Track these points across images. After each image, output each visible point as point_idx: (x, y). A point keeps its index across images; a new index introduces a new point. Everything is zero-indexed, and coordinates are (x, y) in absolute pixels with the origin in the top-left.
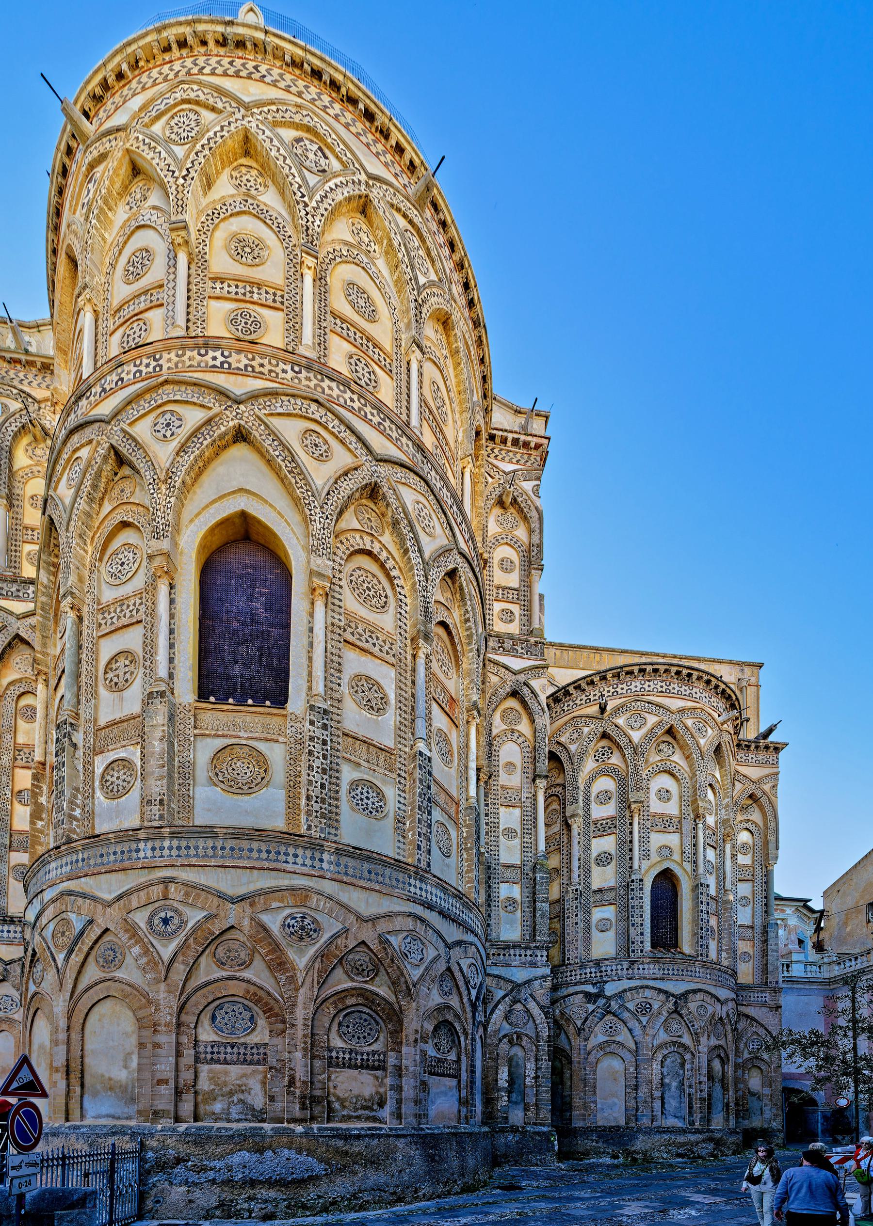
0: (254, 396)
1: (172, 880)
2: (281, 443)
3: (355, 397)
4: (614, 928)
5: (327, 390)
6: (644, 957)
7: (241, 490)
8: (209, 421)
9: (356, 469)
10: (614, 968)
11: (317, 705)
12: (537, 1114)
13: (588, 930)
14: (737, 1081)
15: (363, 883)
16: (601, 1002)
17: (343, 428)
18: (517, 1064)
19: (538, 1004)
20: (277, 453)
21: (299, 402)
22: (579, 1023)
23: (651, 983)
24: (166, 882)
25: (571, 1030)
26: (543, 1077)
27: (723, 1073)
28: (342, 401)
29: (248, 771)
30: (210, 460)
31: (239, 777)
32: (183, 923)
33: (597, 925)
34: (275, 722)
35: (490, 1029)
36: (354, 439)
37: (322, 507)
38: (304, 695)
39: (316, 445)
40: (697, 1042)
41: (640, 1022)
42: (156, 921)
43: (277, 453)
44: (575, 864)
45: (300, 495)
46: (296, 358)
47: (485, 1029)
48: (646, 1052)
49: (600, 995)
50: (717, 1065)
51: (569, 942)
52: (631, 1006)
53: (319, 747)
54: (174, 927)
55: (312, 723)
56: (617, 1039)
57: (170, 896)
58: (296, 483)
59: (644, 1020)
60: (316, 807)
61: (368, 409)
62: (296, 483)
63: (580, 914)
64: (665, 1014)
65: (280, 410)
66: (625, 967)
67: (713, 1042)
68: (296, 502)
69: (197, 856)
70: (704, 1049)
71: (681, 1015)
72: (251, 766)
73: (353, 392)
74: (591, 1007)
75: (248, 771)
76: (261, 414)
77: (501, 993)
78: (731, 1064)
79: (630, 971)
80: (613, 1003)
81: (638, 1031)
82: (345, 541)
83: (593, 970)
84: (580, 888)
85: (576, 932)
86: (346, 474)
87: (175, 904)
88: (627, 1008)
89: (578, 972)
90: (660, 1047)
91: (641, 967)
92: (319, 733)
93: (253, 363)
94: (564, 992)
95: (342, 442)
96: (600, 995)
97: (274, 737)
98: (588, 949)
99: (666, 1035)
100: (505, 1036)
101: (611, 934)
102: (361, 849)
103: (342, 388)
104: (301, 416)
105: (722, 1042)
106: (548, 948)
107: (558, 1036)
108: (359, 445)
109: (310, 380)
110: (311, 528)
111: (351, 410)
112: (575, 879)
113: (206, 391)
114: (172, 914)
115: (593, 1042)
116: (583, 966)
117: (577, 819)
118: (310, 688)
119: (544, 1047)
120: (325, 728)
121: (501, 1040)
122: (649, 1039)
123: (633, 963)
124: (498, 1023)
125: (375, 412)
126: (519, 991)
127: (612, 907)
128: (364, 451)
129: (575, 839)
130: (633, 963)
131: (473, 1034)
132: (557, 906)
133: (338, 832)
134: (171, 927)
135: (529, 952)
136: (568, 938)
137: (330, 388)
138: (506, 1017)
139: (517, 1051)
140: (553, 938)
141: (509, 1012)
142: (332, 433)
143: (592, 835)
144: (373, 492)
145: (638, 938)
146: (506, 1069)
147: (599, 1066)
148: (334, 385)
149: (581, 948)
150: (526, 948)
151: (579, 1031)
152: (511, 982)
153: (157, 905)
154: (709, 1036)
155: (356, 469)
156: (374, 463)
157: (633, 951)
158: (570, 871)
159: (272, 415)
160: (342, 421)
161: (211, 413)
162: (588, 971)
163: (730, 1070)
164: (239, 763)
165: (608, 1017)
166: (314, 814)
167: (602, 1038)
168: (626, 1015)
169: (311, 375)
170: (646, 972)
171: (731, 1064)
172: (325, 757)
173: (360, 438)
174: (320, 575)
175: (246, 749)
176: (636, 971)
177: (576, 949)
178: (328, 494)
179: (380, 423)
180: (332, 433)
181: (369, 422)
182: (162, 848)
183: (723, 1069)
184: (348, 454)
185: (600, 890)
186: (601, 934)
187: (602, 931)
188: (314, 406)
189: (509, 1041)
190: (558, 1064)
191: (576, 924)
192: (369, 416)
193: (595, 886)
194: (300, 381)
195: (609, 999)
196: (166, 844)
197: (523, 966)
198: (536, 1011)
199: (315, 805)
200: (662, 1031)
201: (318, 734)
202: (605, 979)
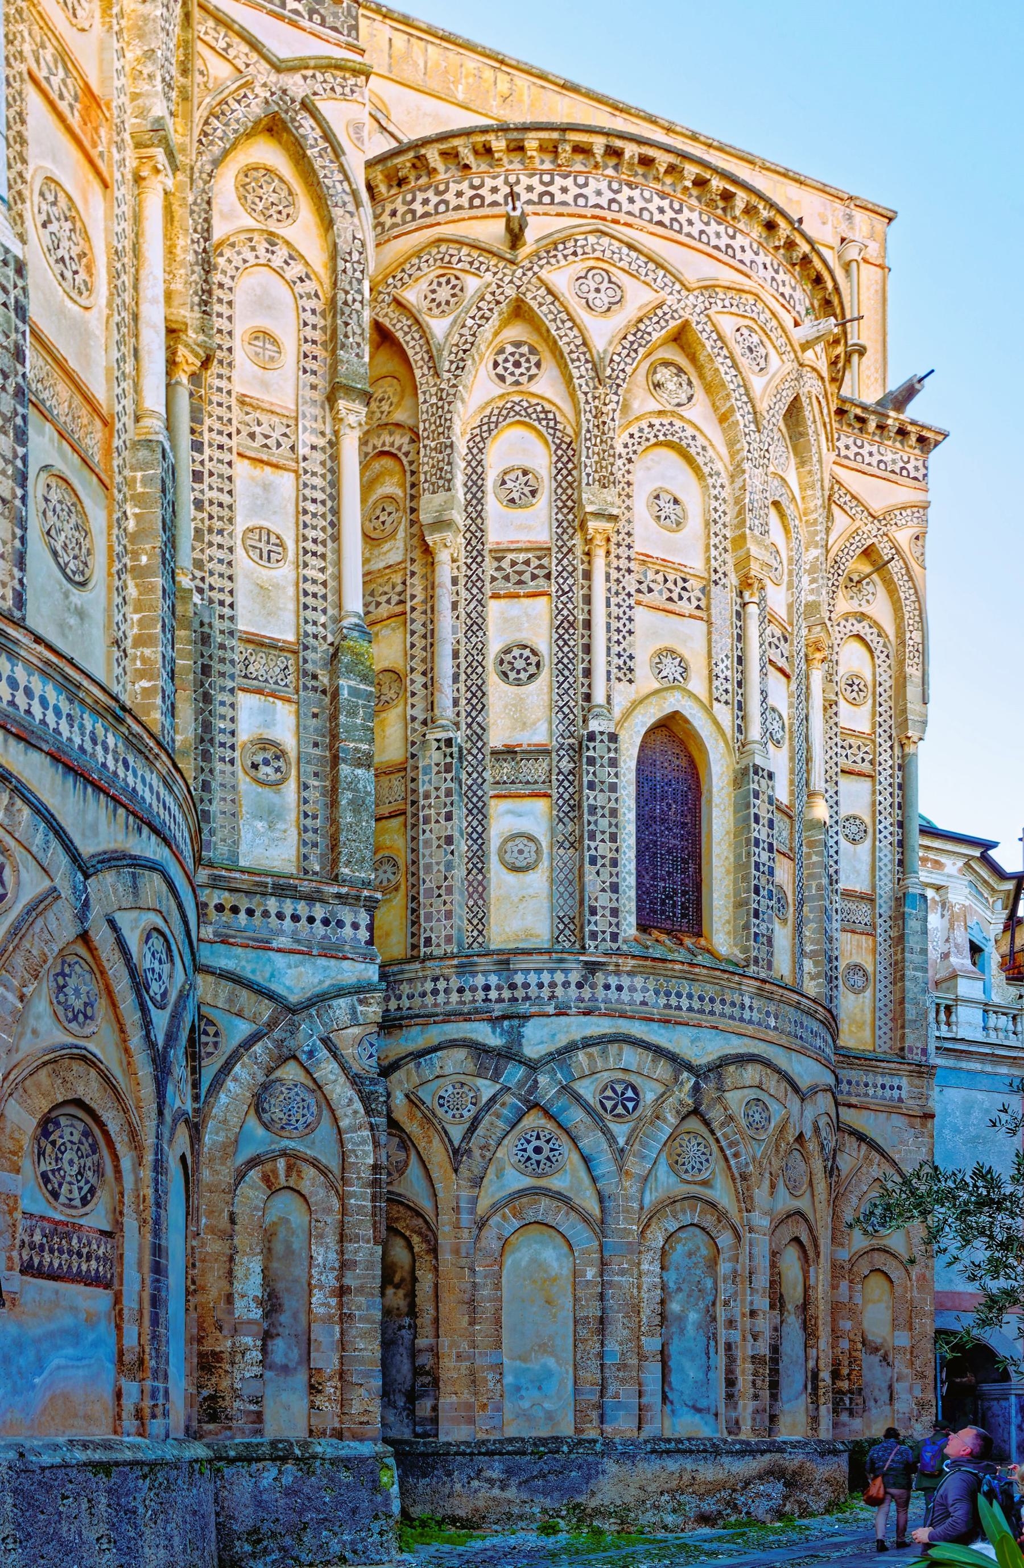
4: (545, 864)
6: (618, 953)
10: (546, 978)
12: (343, 1403)
13: (478, 862)
14: (836, 1308)
16: (514, 1074)
18: (289, 1251)
19: (344, 1068)
22: (456, 1133)
23: (637, 1029)
25: (437, 1154)
26: (360, 1290)
27: (806, 1288)
33: (502, 852)
35: (209, 1138)
40: (746, 1201)
41: (611, 1139)
44: (445, 667)
47: (196, 1131)
48: (625, 1225)
49: (509, 1054)
50: (791, 1262)
51: (429, 892)
52: (587, 1089)
56: (557, 1183)
59: (621, 1131)
63: (460, 813)
64: (672, 1119)
66: (574, 977)
67: (785, 1202)
70: (763, 1222)
71: (707, 1123)
74: (487, 1089)
77: (243, 1029)
78: (824, 1262)
79: (586, 993)
80: (543, 1080)
81: (605, 1165)
83: (493, 980)
84: (459, 737)
85: (449, 866)
88: (578, 1098)
89: (455, 983)
90: (656, 1213)
91: (613, 981)
94: (415, 1039)
96: (509, 1054)
98: (480, 918)
99: (673, 1179)
100: (253, 1162)
101: (538, 880)
105: (803, 1204)
106: (371, 906)
107: (401, 1169)
112: (446, 711)
115: (490, 1194)
116: (465, 968)
117: (449, 535)
119: (360, 1197)
121: (240, 1176)
122: (631, 1187)
123: (592, 968)
124: (234, 1121)
126: (293, 1029)
127: (541, 805)
129: (444, 603)
130: (592, 968)
131: (158, 1150)
132: (396, 783)
135: (319, 912)
136: (429, 881)
138: (258, 1105)
139: (284, 1205)
140: (387, 874)
141: (265, 1087)
143: (488, 590)
145: (604, 900)
146: (256, 1265)
147: (509, 1262)
149: (461, 914)
150: (311, 899)
151: (457, 1154)
152: (271, 996)
154: (773, 1186)
157: (594, 935)
158: (431, 685)
162: (480, 981)
163: (821, 1276)
165: (533, 1120)
167: (516, 1181)
168: (576, 1116)
170: (625, 996)
171: (824, 1262)
176: (600, 993)
177: (449, 915)
183: (806, 1277)
185: (509, 752)
186: (511, 878)
187: (515, 869)
189: (266, 1179)
190: (400, 1254)
191: (449, 840)
193: (496, 739)
195: (533, 1066)
197: (304, 951)
198: (341, 1091)
200: (663, 1169)
202: (524, 1008)
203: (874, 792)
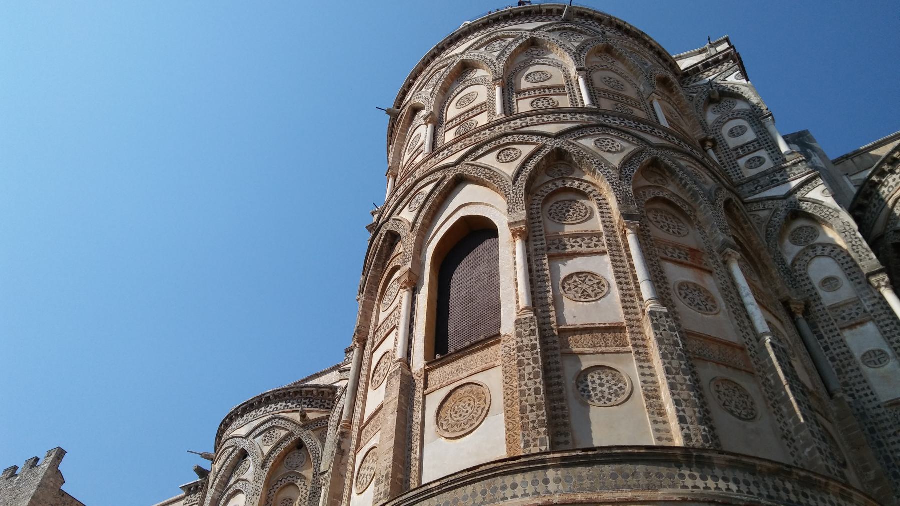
29: (469, 408)
31: (461, 418)
72: (472, 402)
75: (469, 408)
97: (492, 364)
133: (570, 438)
164: (462, 403)
175: (468, 387)
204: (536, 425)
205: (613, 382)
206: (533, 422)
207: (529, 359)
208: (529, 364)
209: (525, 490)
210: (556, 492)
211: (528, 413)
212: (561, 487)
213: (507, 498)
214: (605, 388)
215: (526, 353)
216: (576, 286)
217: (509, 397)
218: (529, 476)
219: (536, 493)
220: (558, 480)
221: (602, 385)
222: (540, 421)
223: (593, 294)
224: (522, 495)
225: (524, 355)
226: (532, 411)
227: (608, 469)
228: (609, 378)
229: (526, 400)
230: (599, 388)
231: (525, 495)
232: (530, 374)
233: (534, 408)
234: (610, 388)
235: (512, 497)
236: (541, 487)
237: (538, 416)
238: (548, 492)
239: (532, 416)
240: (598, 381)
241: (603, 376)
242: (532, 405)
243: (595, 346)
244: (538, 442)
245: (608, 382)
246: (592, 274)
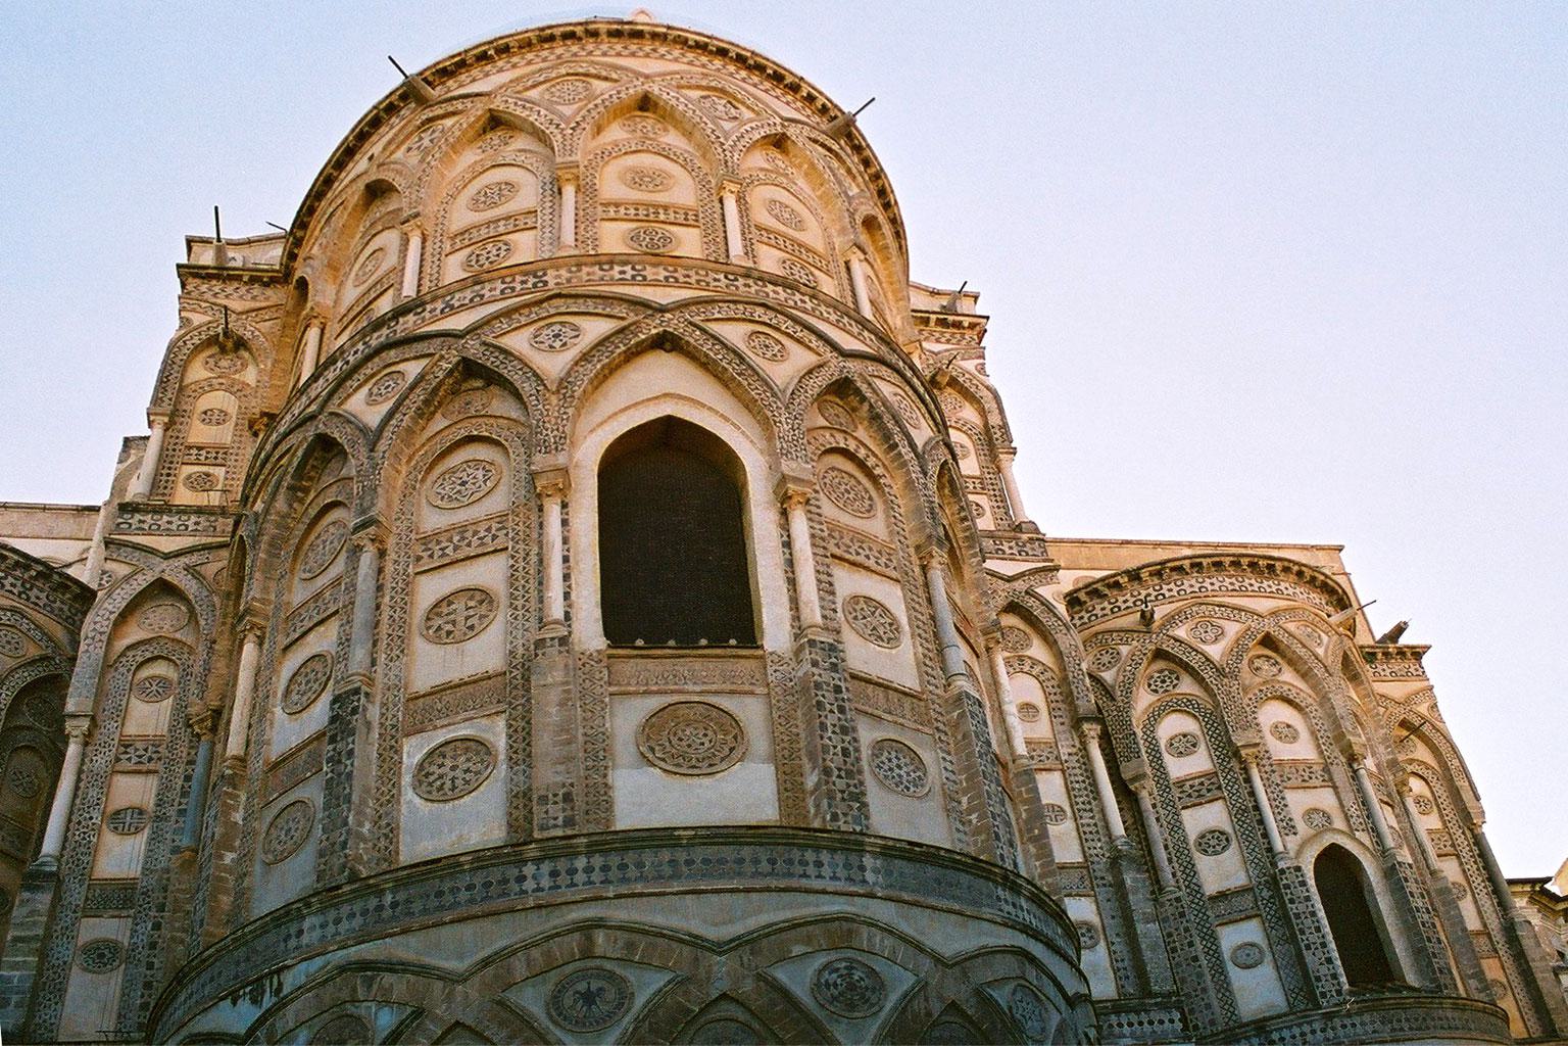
0: (683, 305)
1: (599, 924)
2: (725, 346)
3: (807, 299)
5: (771, 294)
7: (666, 395)
8: (622, 330)
9: (821, 366)
11: (818, 638)
15: (932, 901)
17: (799, 328)
20: (720, 357)
21: (740, 307)
24: (587, 927)
28: (791, 303)
30: (619, 366)
32: (625, 997)
34: (746, 666)
36: (813, 338)
37: (787, 408)
38: (789, 628)
39: (767, 346)
42: (568, 1001)
43: (720, 357)
45: (757, 397)
46: (729, 269)
53: (830, 696)
54: (605, 1008)
55: (815, 664)
57: (598, 951)
58: (749, 384)
60: (841, 784)
61: (823, 308)
62: (749, 384)
65: (717, 316)
68: (749, 405)
69: (642, 878)
73: (803, 294)
76: (697, 319)
82: (812, 441)
86: (810, 372)
87: (608, 965)
92: (826, 677)
93: (675, 275)
95: (798, 341)
102: (920, 845)
103: (789, 291)
104: (744, 320)
108: (821, 343)
109: (750, 287)
110: (776, 430)
111: (805, 311)
113: (615, 302)
114: (601, 984)
118: (797, 618)
120: (834, 667)
125: (831, 310)
128: (828, 349)
134: (601, 1007)
137: (775, 292)
142: (788, 335)
144: (843, 388)
148: (779, 289)
153: (569, 969)
155: (821, 366)
156: (841, 359)
159: (708, 320)
160: (796, 321)
161: (625, 323)
166: (839, 795)
169: (751, 282)
172: (842, 710)
173: (821, 336)
174: (796, 480)
178: (793, 393)
179: (838, 321)
180: (788, 335)
181: (826, 320)
182: (572, 872)
184: (810, 353)
188: (760, 311)
192: (825, 315)
194: (737, 288)
196: (581, 863)
199: (838, 781)
201: (826, 677)
203: (1461, 864)
204: (845, 795)
205: (912, 768)
206: (843, 792)
207: (832, 704)
208: (831, 711)
209: (835, 873)
210: (874, 884)
211: (834, 778)
212: (881, 879)
213: (809, 877)
214: (902, 773)
215: (827, 694)
216: (864, 618)
217: (785, 745)
218: (840, 858)
219: (849, 879)
220: (876, 871)
221: (899, 767)
222: (850, 793)
223: (885, 637)
224: (831, 878)
225: (823, 696)
226: (839, 777)
227: (932, 871)
228: (908, 760)
229: (832, 761)
230: (897, 771)
231: (834, 878)
232: (834, 726)
233: (843, 774)
234: (908, 774)
235: (817, 877)
236: (855, 874)
237: (848, 785)
238: (864, 881)
239: (841, 784)
240: (895, 761)
241: (900, 756)
242: (839, 770)
243: (890, 713)
244: (849, 818)
245: (906, 765)
246: (886, 610)
